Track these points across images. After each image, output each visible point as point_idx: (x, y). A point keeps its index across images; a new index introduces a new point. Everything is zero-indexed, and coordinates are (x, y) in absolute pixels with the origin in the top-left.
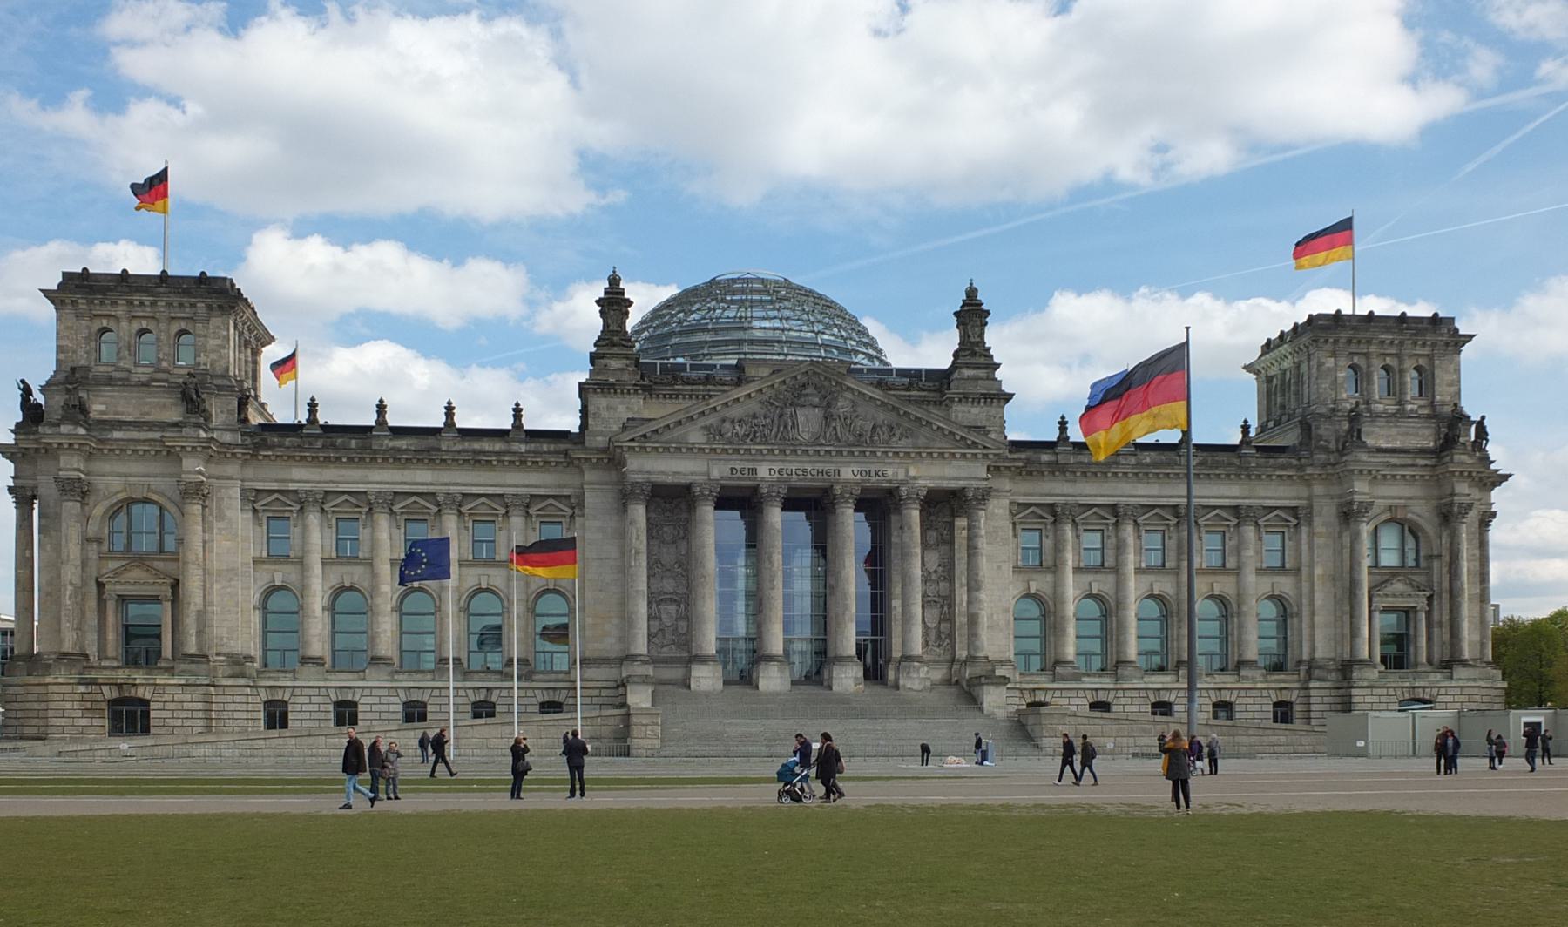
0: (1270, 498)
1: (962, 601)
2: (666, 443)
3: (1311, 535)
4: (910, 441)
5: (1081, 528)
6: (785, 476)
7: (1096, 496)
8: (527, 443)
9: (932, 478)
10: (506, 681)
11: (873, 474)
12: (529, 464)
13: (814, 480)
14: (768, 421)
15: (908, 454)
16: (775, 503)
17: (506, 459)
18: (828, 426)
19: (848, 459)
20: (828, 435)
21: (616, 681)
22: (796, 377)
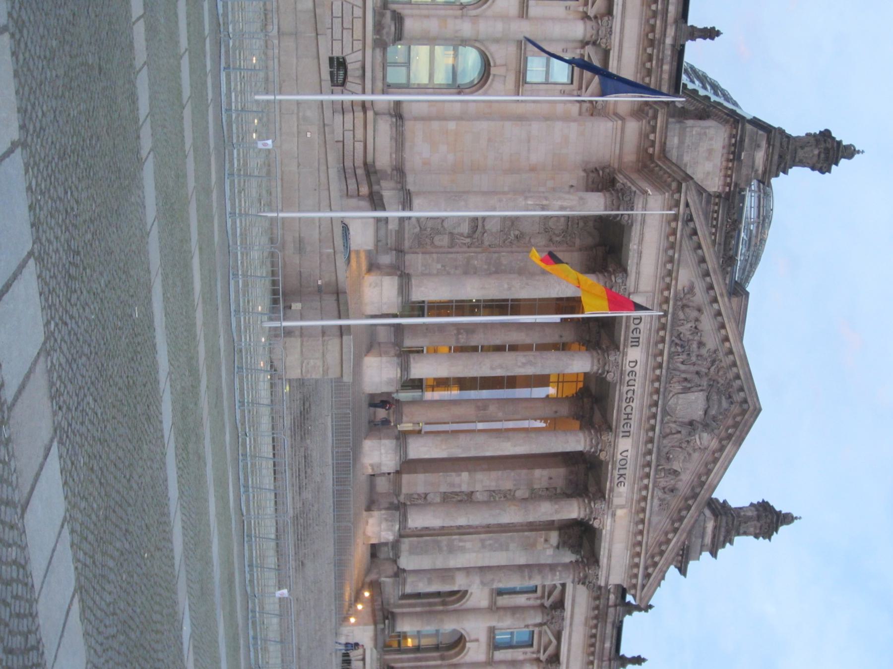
1: (465, 541)
2: (681, 246)
4: (656, 508)
5: (536, 630)
6: (627, 378)
7: (570, 644)
8: (673, 46)
9: (612, 532)
10: (374, 16)
11: (622, 472)
12: (649, 50)
13: (618, 410)
14: (694, 359)
15: (643, 510)
16: (595, 368)
17: (658, 23)
18: (683, 424)
19: (642, 449)
20: (673, 425)
22: (741, 389)
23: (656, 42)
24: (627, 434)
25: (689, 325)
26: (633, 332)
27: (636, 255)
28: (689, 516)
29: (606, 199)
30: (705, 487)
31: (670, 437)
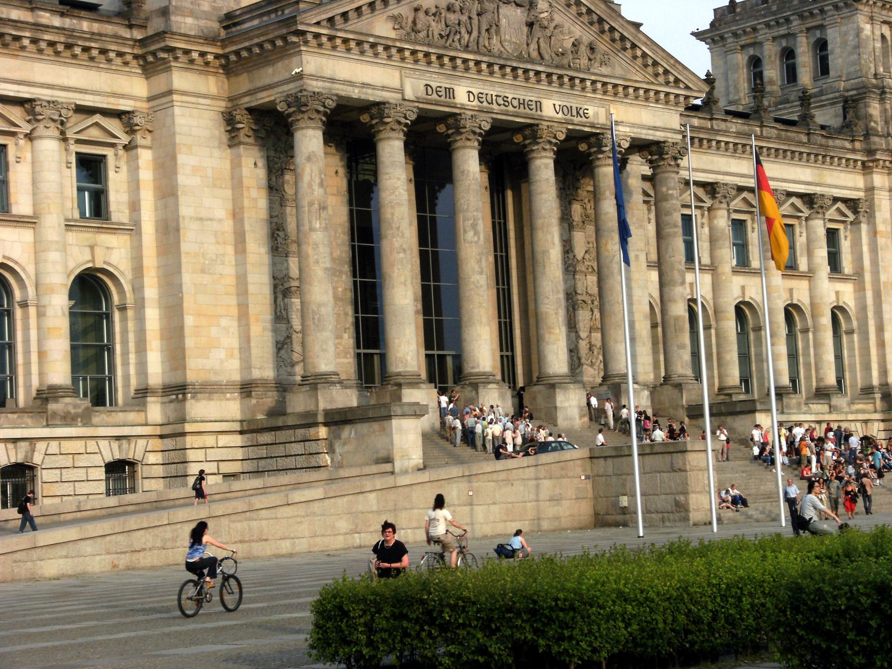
0: (836, 187)
2: (362, 34)
3: (874, 233)
4: (609, 69)
6: (485, 104)
9: (633, 125)
11: (574, 113)
17: (47, 37)
19: (555, 87)
21: (249, 422)
23: (70, 41)
24: (539, 105)
25: (433, 24)
26: (440, 96)
27: (364, 90)
28: (621, 30)
29: (307, 128)
30: (593, 8)
31: (543, 52)
